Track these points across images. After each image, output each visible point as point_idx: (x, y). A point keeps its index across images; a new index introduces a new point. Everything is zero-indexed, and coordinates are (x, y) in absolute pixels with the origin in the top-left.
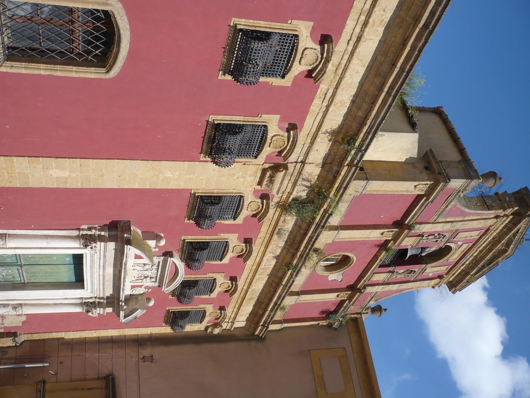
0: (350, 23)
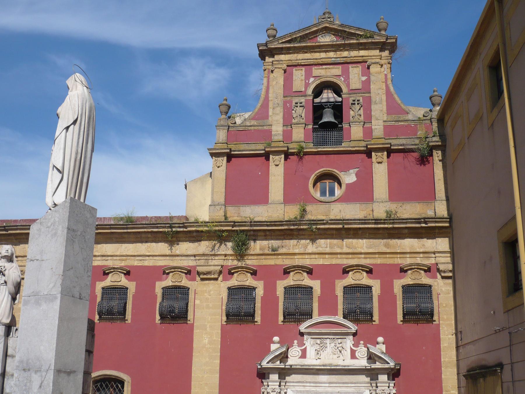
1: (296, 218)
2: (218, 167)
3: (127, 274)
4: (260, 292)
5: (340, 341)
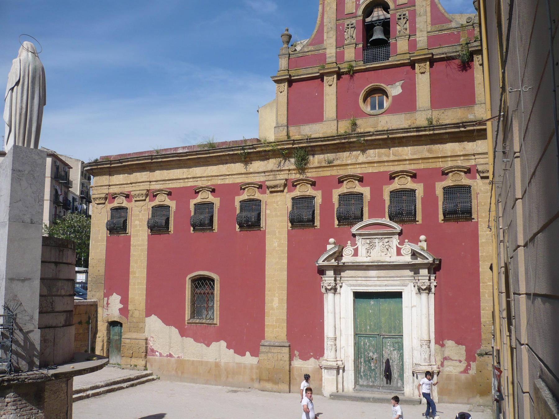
0: (189, 184)
1: (346, 132)
2: (281, 92)
3: (213, 191)
4: (318, 201)
5: (386, 240)
